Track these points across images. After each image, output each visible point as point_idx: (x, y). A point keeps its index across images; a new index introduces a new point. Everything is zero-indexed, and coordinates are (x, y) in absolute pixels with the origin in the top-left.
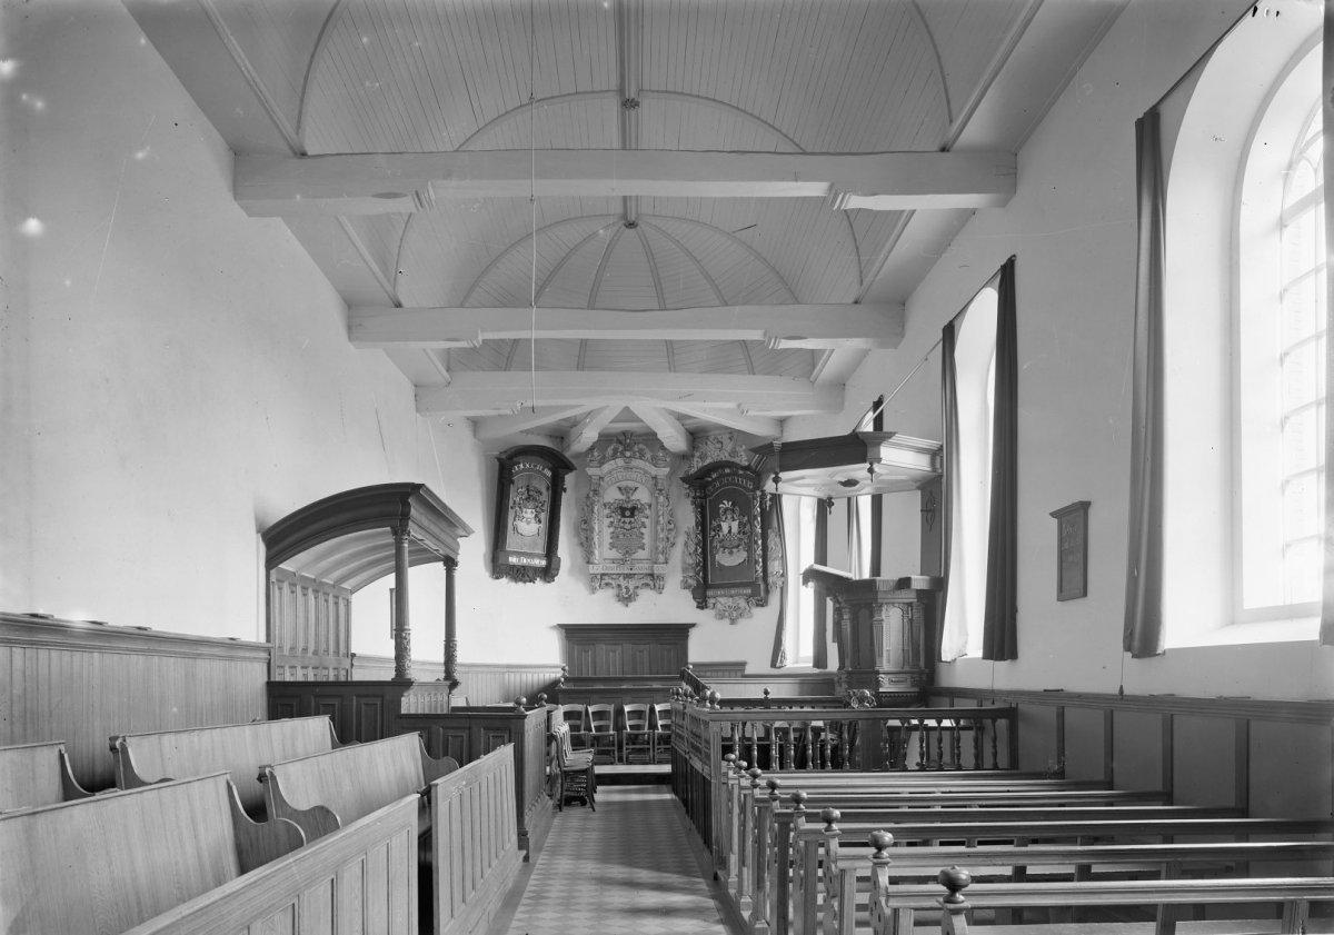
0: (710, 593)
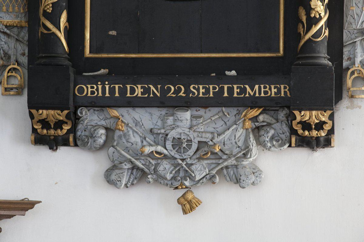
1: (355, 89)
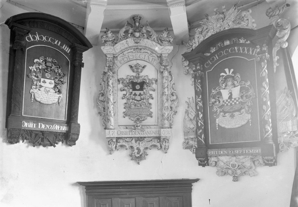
0: (210, 152)
1: (282, 149)
